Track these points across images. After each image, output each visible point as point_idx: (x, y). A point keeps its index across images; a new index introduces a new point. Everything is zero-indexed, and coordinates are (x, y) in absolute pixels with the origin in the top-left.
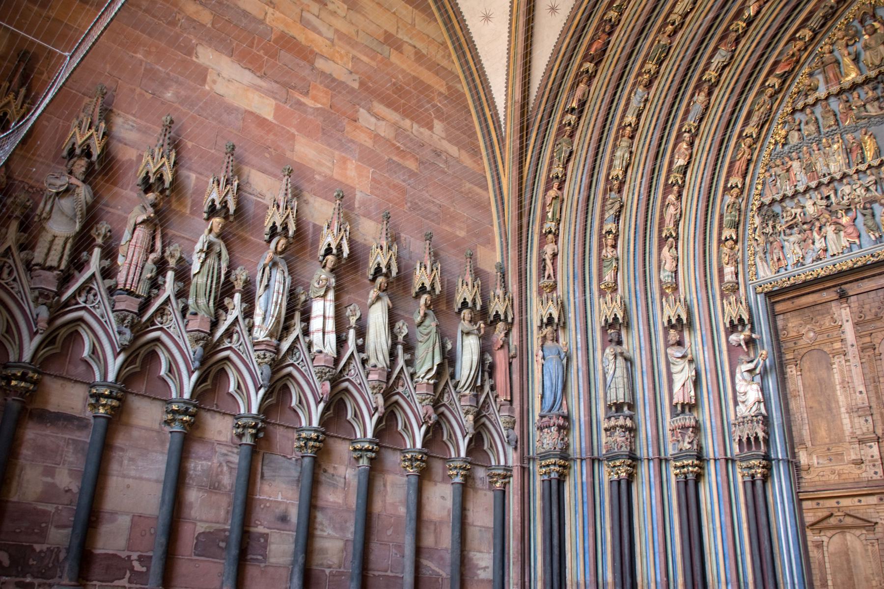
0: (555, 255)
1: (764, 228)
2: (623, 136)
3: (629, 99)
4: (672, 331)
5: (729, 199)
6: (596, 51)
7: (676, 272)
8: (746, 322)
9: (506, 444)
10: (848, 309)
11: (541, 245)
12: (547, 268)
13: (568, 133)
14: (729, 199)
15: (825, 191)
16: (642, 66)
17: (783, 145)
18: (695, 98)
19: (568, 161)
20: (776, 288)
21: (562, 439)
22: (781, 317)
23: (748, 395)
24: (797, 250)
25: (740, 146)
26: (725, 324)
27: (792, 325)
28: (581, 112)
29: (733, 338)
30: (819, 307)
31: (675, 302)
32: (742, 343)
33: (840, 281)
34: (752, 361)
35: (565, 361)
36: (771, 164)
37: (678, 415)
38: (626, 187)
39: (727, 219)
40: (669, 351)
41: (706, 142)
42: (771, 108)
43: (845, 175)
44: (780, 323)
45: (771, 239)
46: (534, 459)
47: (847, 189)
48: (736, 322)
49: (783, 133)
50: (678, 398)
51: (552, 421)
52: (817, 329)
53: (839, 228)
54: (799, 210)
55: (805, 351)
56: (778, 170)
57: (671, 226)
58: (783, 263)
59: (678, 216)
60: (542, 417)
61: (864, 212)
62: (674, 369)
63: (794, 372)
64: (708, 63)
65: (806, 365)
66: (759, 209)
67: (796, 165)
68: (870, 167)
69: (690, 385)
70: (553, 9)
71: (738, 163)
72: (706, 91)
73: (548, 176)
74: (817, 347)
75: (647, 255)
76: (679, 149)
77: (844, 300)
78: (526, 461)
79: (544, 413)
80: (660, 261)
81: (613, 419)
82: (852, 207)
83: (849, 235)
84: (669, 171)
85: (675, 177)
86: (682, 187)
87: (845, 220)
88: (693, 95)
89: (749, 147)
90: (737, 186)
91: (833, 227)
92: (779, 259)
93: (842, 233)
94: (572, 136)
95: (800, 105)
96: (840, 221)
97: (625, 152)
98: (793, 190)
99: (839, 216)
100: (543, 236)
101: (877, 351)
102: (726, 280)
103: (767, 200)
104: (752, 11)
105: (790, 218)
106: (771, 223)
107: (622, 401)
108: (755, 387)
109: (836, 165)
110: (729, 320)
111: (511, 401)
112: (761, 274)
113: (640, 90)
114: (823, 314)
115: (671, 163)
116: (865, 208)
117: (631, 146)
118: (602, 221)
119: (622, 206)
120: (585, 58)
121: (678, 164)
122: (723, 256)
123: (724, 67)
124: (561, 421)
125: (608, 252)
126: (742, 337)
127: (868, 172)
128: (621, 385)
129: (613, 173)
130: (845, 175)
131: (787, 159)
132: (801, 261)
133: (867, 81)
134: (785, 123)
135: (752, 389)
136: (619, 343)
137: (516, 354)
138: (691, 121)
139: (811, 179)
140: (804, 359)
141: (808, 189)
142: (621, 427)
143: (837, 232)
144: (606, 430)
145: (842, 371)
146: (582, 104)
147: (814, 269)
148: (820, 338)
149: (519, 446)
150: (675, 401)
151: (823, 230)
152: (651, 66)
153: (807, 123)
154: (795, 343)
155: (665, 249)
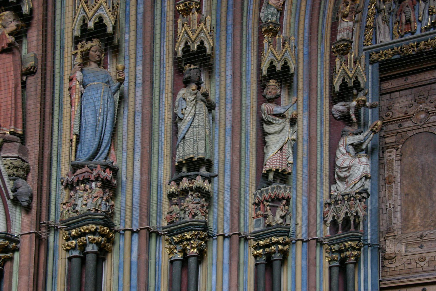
8: (362, 86)
9: (9, 202)
46: (57, 229)
48: (351, 84)
60: (75, 167)
69: (288, 149)
78: (43, 230)
79: (82, 160)
111: (23, 138)
124: (108, 175)
128: (202, 136)
144: (171, 196)
149: (34, 205)
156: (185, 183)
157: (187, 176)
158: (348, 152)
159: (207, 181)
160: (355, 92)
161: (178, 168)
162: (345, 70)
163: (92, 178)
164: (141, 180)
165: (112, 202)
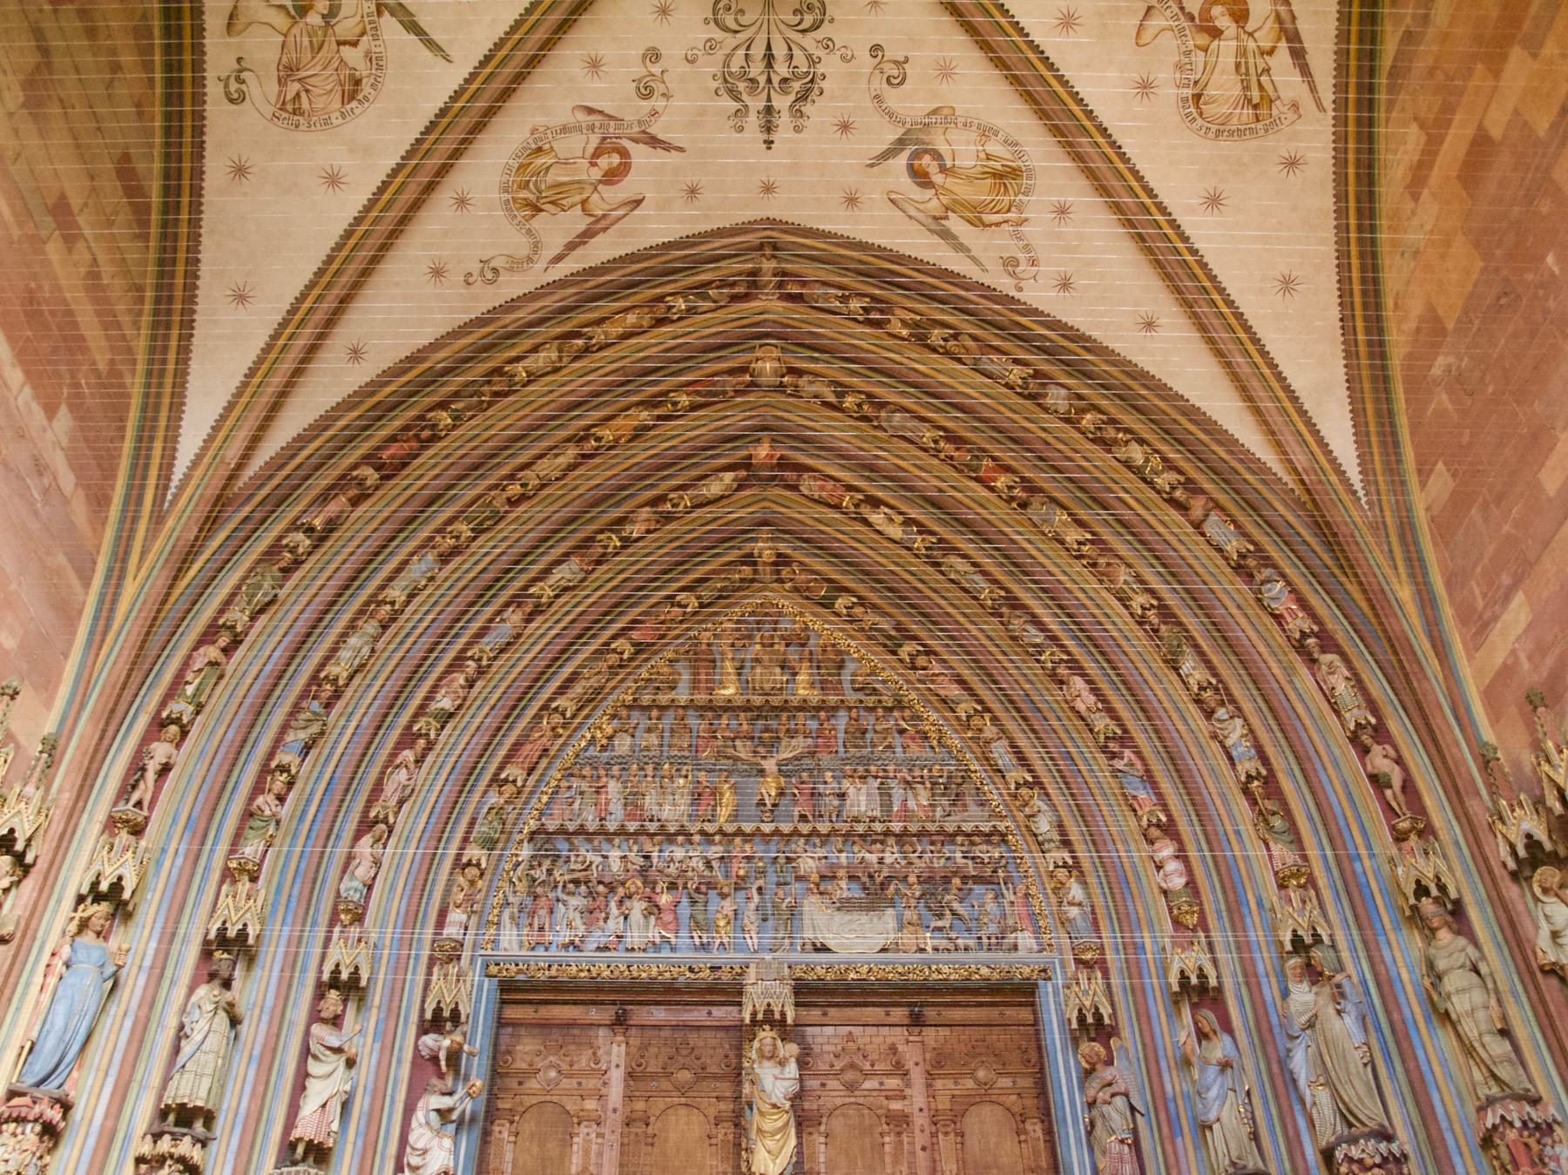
0: (165, 769)
1: (532, 867)
2: (372, 616)
3: (406, 562)
4: (333, 995)
5: (494, 799)
6: (392, 457)
7: (370, 888)
8: (463, 1018)
10: (623, 1046)
11: (147, 739)
12: (142, 785)
13: (283, 564)
14: (494, 799)
15: (648, 847)
16: (450, 521)
17: (604, 748)
18: (505, 615)
19: (262, 611)
20: (521, 977)
21: (41, 1158)
22: (510, 1030)
23: (428, 1157)
24: (578, 922)
25: (542, 718)
26: (422, 1010)
27: (526, 1049)
28: (323, 539)
29: (429, 1040)
30: (576, 1031)
31: (359, 940)
32: (442, 1056)
33: (623, 998)
34: (450, 1094)
35: (110, 984)
36: (575, 772)
37: (295, 1163)
38: (340, 704)
39: (481, 829)
40: (316, 1029)
41: (492, 691)
43: (683, 831)
44: (505, 1040)
45: (539, 890)
47: (679, 853)
48: (446, 1014)
49: (609, 730)
50: (306, 1128)
51: (37, 1109)
52: (565, 1067)
53: (654, 909)
54: (600, 859)
55: (534, 1100)
56: (584, 785)
57: (393, 802)
58: (549, 936)
59: (408, 791)
61: (695, 895)
62: (313, 1067)
63: (505, 1134)
64: (547, 571)
65: (528, 1126)
66: (532, 836)
67: (613, 787)
69: (335, 1108)
70: (356, 354)
71: (529, 747)
72: (528, 609)
73: (216, 619)
74: (555, 1099)
75: (333, 837)
76: (452, 681)
77: (619, 1029)
80: (350, 858)
81: (167, 1138)
82: (680, 882)
83: (665, 926)
84: (421, 711)
85: (428, 723)
86: (429, 747)
87: (664, 899)
88: (507, 605)
89: (553, 729)
90: (514, 781)
91: (644, 905)
92: (541, 929)
93: (653, 918)
94: (287, 571)
95: (646, 699)
97: (366, 643)
99: (658, 890)
100: (159, 724)
101: (650, 1130)
102: (446, 931)
103: (552, 825)
104: (636, 530)
106: (547, 864)
107: (200, 1103)
108: (448, 1143)
109: (673, 809)
110: (434, 1005)
112: (504, 943)
113: (431, 557)
114: (580, 1044)
115: (429, 698)
116: (697, 890)
117: (376, 639)
118: (278, 741)
119: (322, 733)
120: (368, 459)
121: (440, 705)
122: (455, 889)
123: (566, 589)
124: (54, 1114)
125: (265, 802)
126: (446, 1043)
127: (717, 838)
128: (209, 1071)
129: (332, 669)
130: (683, 831)
131: (602, 772)
133: (747, 708)
134: (613, 717)
135: (441, 1147)
136: (227, 984)
137: (12, 936)
138: (488, 644)
139: (630, 817)
140: (527, 1115)
141: (622, 832)
142: (182, 1160)
143: (647, 914)
144: (140, 1160)
145: (587, 1151)
146: (332, 526)
147: (591, 962)
148: (565, 1083)
150: (296, 1134)
151: (628, 903)
152: (464, 529)
153: (649, 730)
154: (520, 1083)
155: (367, 840)
156: (165, 1145)
157: (171, 1133)
158: (427, 1123)
159: (199, 1145)
160: (449, 1025)
161: (163, 1114)
162: (444, 991)
163: (31, 1117)
164: (102, 1126)
165: (47, 1159)
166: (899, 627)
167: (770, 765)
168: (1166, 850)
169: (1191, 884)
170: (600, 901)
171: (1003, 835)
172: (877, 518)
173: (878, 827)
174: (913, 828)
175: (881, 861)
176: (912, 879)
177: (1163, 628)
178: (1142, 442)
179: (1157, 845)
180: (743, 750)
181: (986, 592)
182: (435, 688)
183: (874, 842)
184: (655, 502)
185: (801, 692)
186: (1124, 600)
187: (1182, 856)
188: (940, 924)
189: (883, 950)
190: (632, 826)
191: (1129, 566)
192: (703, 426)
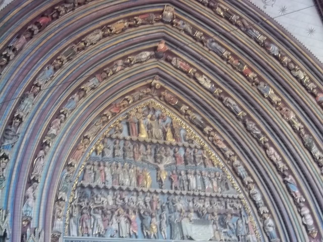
16: (58, 54)
18: (73, 96)
24: (102, 225)
42: (100, 129)
43: (135, 190)
68: (149, 191)
76: (56, 122)
83: (134, 227)
87: (133, 217)
88: (73, 93)
91: (126, 219)
92: (87, 228)
96: (130, 217)
98: (103, 185)
99: (130, 213)
105: (99, 202)
106: (86, 201)
109: (128, 181)
116: (144, 213)
130: (135, 190)
132: (101, 233)
166: (203, 119)
167: (161, 166)
168: (306, 211)
169: (315, 224)
170: (109, 217)
171: (240, 199)
172: (201, 79)
173: (202, 194)
174: (214, 195)
175: (204, 206)
176: (216, 214)
177: (306, 136)
178: (303, 71)
179: (303, 209)
180: (150, 159)
181: (240, 113)
182: (50, 125)
183: (200, 199)
184: (124, 58)
185: (169, 139)
186: (290, 123)
187: (311, 213)
188: (225, 230)
189: (211, 240)
190: (117, 187)
191: (294, 112)
192: (141, 33)
